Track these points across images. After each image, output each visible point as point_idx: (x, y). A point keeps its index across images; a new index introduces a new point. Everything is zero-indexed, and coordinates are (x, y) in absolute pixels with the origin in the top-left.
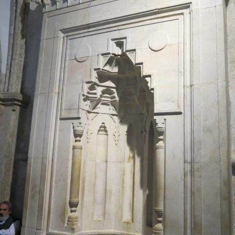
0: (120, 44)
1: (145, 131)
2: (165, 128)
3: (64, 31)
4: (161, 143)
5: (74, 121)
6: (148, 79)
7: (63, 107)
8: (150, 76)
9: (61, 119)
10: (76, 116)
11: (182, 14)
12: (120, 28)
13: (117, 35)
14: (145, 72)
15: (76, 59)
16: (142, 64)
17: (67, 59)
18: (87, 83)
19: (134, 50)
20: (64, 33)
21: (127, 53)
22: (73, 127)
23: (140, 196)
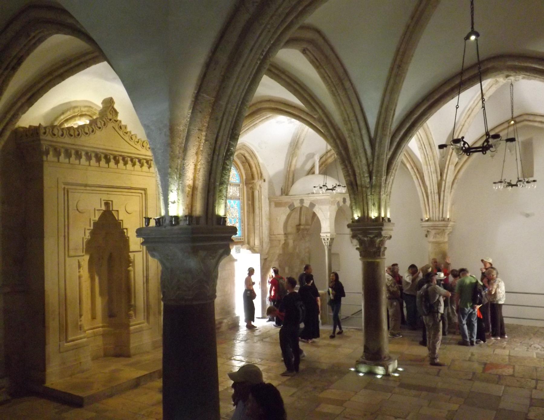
0: (107, 204)
1: (103, 258)
2: (134, 259)
3: (65, 184)
4: (130, 268)
5: (79, 258)
6: (125, 231)
7: (71, 247)
8: (127, 229)
9: (69, 256)
10: (82, 254)
11: (141, 193)
12: (109, 192)
13: (105, 197)
14: (124, 227)
15: (77, 210)
16: (122, 220)
17: (70, 209)
18: (88, 230)
19: (118, 211)
20: (64, 184)
21: (113, 212)
22: (79, 262)
23: (99, 302)
